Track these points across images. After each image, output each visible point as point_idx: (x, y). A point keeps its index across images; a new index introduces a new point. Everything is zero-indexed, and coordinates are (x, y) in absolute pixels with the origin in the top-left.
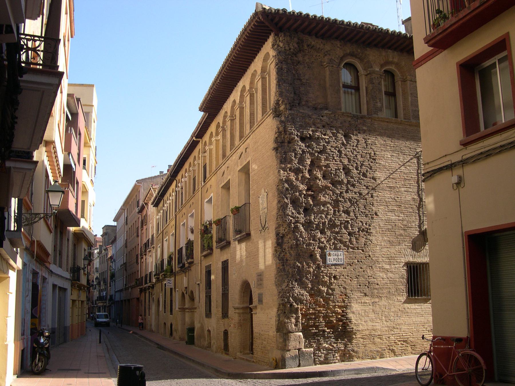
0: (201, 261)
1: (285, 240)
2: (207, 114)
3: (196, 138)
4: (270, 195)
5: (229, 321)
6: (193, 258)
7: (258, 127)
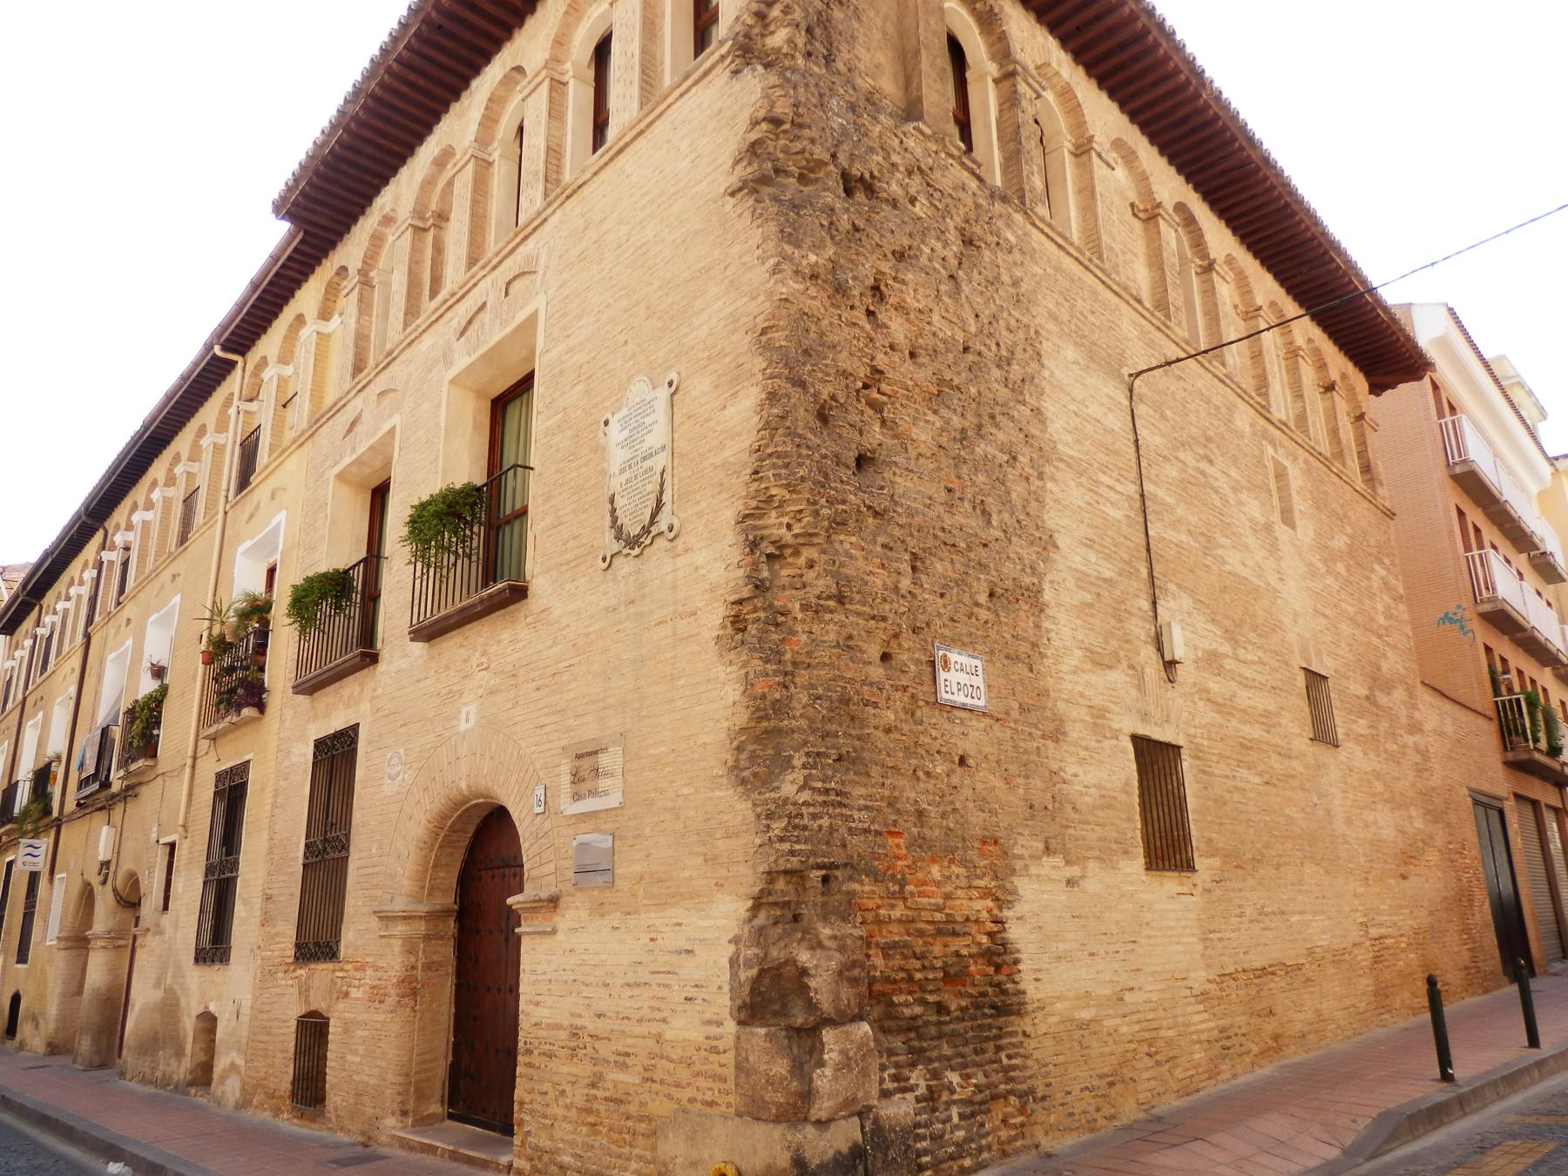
0: (195, 758)
1: (784, 572)
3: (224, 348)
4: (700, 386)
5: (340, 974)
6: (154, 756)
7: (612, 159)
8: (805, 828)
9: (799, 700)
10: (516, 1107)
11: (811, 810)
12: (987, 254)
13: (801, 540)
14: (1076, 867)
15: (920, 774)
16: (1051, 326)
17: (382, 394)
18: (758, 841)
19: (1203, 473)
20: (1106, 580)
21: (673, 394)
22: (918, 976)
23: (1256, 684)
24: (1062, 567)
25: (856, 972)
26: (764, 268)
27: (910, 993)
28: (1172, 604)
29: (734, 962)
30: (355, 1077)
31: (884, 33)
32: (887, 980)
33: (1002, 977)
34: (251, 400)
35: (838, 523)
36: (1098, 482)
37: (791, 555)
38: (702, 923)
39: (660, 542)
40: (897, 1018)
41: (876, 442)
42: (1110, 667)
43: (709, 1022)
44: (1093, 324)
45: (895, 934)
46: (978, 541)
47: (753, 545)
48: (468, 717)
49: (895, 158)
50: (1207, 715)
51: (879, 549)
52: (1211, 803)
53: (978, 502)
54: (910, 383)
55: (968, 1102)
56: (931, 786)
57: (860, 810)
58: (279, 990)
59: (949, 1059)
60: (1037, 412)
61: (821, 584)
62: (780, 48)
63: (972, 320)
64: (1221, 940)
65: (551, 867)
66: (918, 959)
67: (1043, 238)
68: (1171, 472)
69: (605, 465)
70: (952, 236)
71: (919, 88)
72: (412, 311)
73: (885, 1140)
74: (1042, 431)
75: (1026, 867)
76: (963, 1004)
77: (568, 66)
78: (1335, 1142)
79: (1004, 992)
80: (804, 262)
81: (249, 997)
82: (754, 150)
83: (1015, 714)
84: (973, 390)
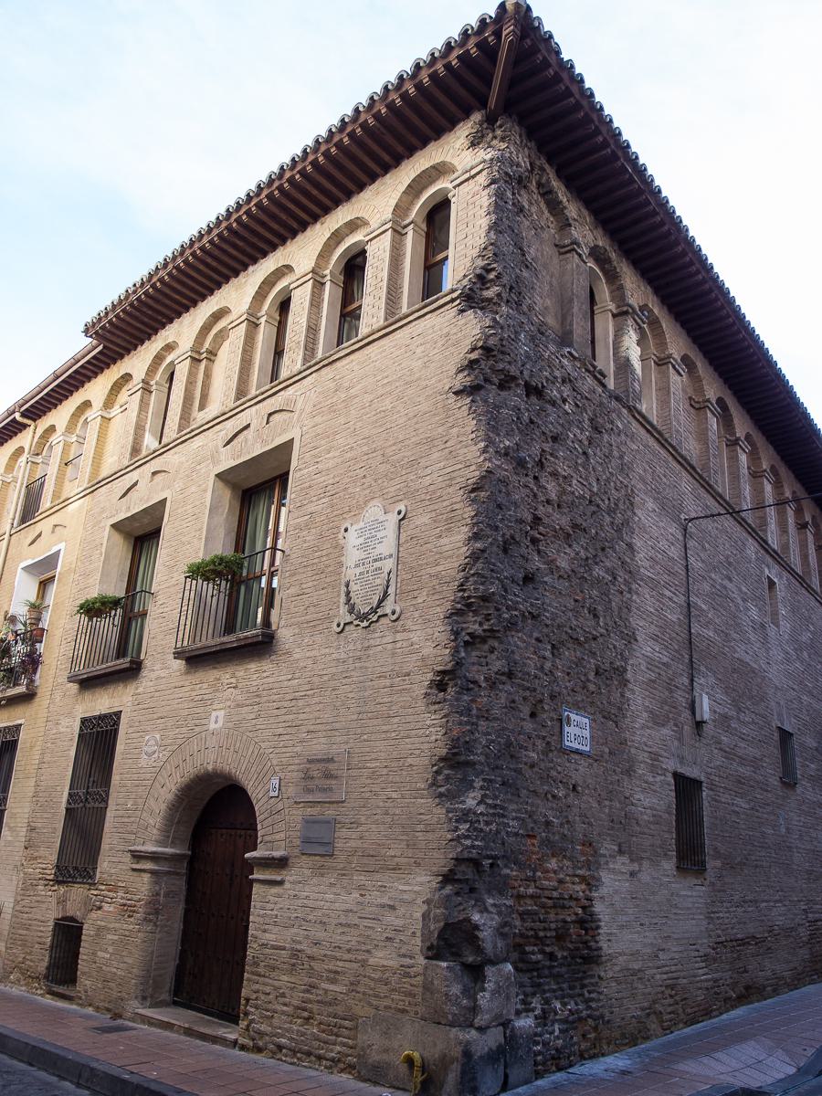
1: (474, 654)
2: (101, 347)
3: (23, 415)
8: (481, 830)
9: (480, 743)
10: (243, 1002)
11: (485, 818)
12: (606, 436)
13: (489, 634)
14: (636, 864)
15: (549, 796)
16: (640, 486)
17: (154, 474)
18: (449, 837)
19: (725, 588)
20: (664, 664)
21: (400, 520)
22: (541, 934)
23: (750, 738)
24: (638, 655)
25: (507, 929)
26: (476, 448)
27: (535, 945)
28: (702, 681)
29: (425, 916)
30: (104, 968)
31: (551, 285)
32: (522, 935)
33: (588, 938)
34: (37, 454)
35: (512, 625)
36: (662, 595)
37: (480, 643)
38: (401, 887)
39: (383, 620)
40: (528, 962)
41: (535, 567)
42: (663, 725)
43: (404, 956)
44: (665, 484)
45: (530, 906)
46: (591, 637)
47: (456, 633)
48: (217, 720)
49: (557, 374)
50: (719, 760)
51: (534, 641)
52: (718, 822)
53: (592, 609)
54: (558, 527)
55: (565, 1021)
56: (555, 805)
57: (513, 819)
58: (39, 898)
59: (554, 991)
60: (630, 546)
61: (498, 665)
62: (493, 298)
63: (595, 484)
64: (718, 918)
65: (282, 835)
66: (540, 922)
67: (639, 426)
68: (706, 587)
69: (343, 559)
70: (586, 424)
71: (571, 325)
72: (185, 416)
73: (517, 1043)
74: (632, 559)
75: (607, 863)
76: (565, 954)
77: (327, 272)
78: (793, 1063)
79: (589, 948)
80: (502, 446)
81: (12, 900)
82: (472, 365)
83: (606, 756)
84: (593, 531)
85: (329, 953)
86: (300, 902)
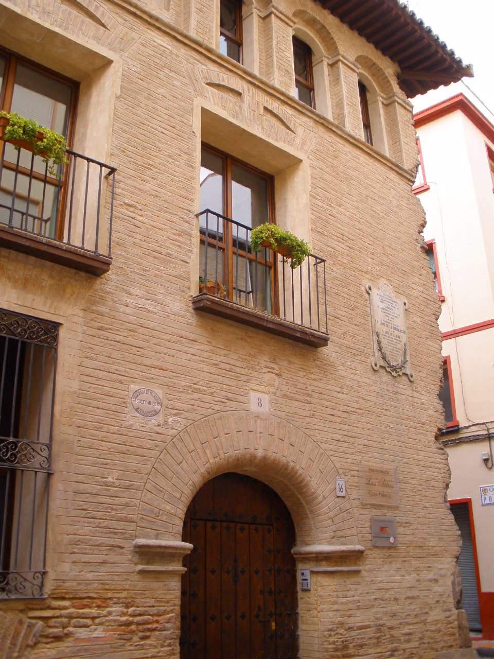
29: (453, 583)
43: (446, 611)
85: (403, 621)
86: (375, 587)
